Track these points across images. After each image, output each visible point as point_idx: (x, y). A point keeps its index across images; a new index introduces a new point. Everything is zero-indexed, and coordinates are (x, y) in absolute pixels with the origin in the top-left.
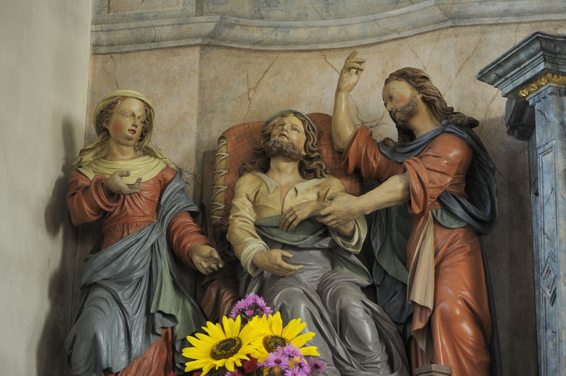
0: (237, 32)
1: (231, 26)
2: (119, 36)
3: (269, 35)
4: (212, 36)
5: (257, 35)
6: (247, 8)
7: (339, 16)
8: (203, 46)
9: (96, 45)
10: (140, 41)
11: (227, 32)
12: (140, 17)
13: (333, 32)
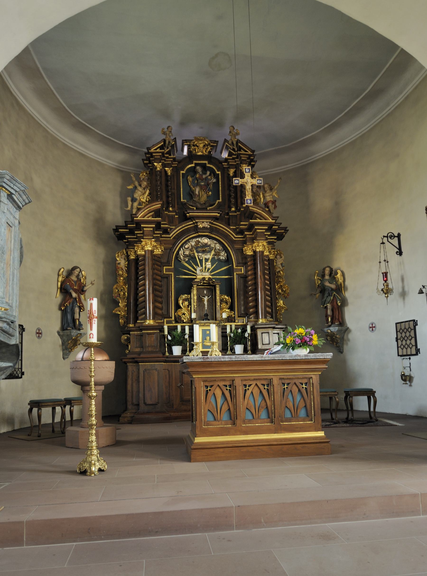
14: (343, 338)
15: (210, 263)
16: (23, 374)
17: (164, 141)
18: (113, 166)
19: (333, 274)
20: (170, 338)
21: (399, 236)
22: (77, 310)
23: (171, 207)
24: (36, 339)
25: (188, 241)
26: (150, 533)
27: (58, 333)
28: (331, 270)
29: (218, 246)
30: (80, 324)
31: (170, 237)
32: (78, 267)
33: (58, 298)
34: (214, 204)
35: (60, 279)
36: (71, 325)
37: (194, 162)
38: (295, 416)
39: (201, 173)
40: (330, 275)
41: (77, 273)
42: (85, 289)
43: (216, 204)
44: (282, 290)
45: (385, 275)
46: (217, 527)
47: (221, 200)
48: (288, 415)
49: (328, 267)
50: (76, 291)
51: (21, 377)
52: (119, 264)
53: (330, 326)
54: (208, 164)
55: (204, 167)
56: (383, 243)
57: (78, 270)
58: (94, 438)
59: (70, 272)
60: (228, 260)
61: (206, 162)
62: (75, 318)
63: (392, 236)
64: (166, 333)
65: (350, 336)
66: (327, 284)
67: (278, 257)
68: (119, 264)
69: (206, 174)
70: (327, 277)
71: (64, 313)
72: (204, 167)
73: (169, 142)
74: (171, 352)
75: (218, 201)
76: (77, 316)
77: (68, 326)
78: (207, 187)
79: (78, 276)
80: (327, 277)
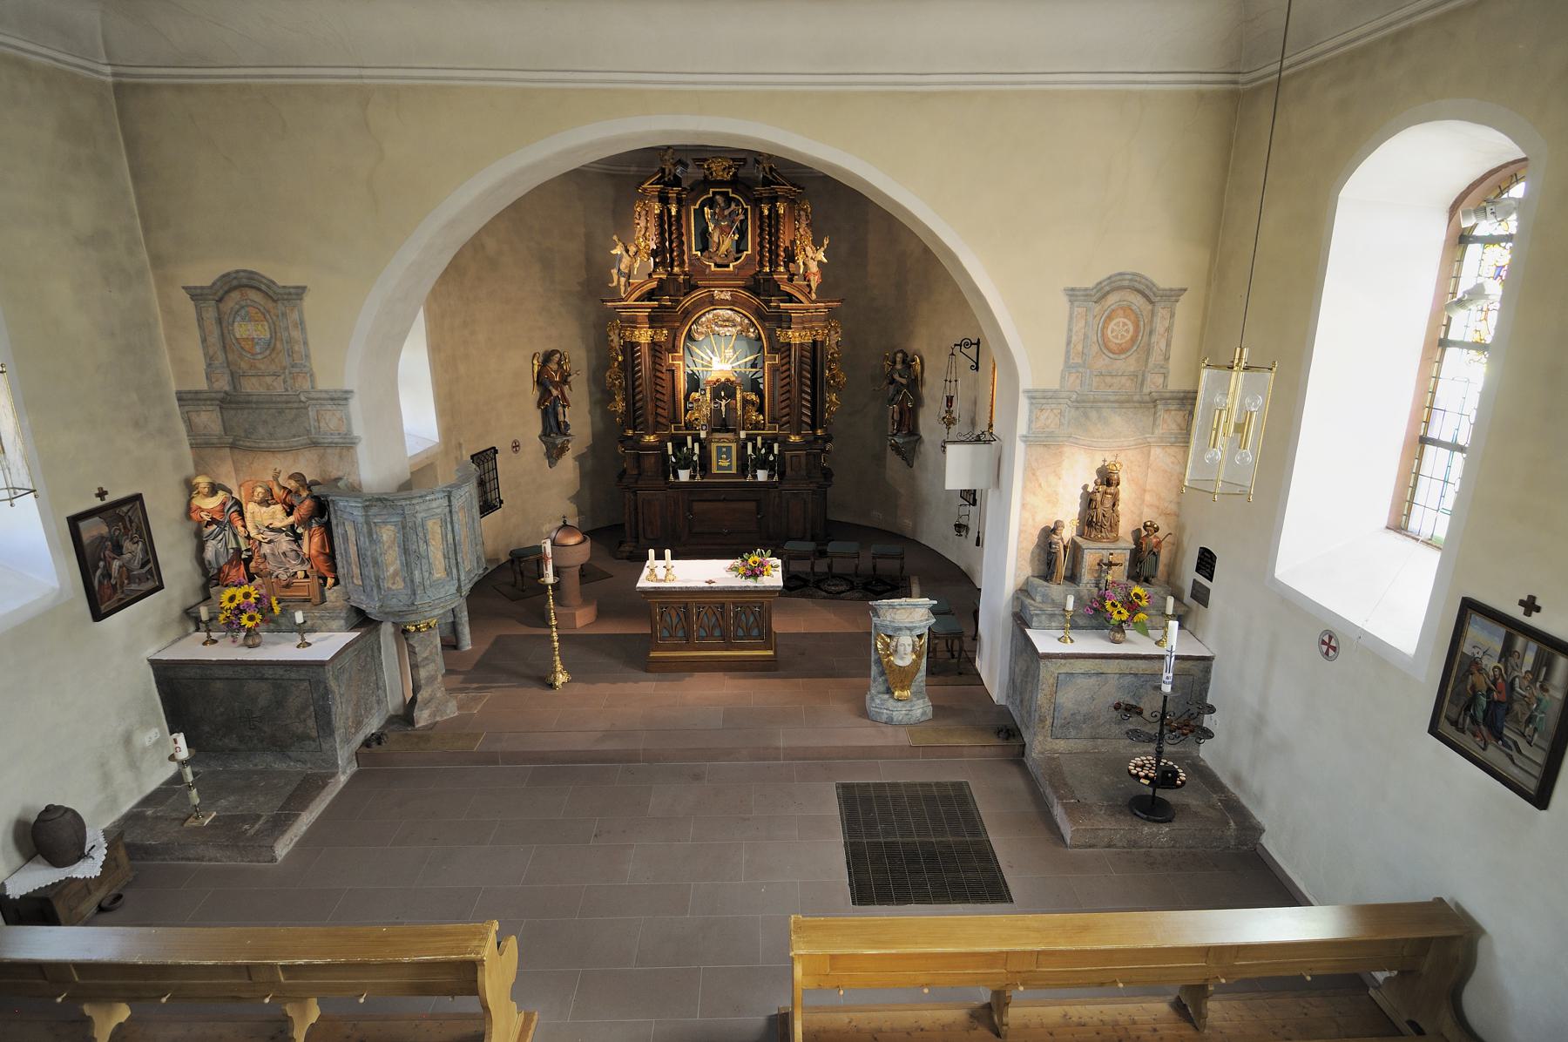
0: (241, 443)
1: (239, 440)
2: (199, 441)
3: (253, 445)
4: (232, 443)
5: (248, 444)
6: (243, 435)
7: (276, 439)
8: (231, 448)
9: (190, 444)
10: (206, 444)
11: (237, 443)
12: (205, 435)
13: (275, 445)
14: (914, 449)
15: (731, 351)
16: (501, 502)
17: (663, 171)
18: (599, 171)
19: (907, 363)
20: (674, 460)
21: (978, 344)
22: (560, 409)
23: (678, 266)
24: (514, 454)
25: (704, 314)
26: (581, 762)
27: (540, 437)
28: (905, 355)
29: (746, 321)
30: (567, 425)
31: (677, 312)
32: (558, 351)
33: (533, 394)
34: (740, 258)
35: (536, 371)
36: (555, 430)
37: (711, 190)
38: (749, 636)
39: (722, 205)
40: (904, 361)
41: (557, 359)
42: (569, 379)
43: (743, 258)
44: (834, 381)
45: (950, 400)
46: (629, 761)
47: (749, 252)
48: (740, 632)
49: (902, 351)
50: (556, 385)
51: (500, 507)
52: (612, 341)
53: (895, 435)
54: (733, 193)
55: (725, 194)
56: (953, 354)
57: (558, 355)
58: (558, 658)
59: (548, 357)
60: (759, 338)
61: (730, 190)
62: (560, 420)
63: (969, 344)
64: (670, 452)
65: (922, 449)
66: (896, 377)
67: (832, 332)
68: (612, 341)
69: (730, 207)
70: (899, 366)
71: (545, 414)
72: (725, 194)
73: (670, 170)
74: (676, 476)
75: (745, 253)
76: (561, 418)
77: (551, 431)
78: (732, 228)
79: (559, 363)
80: (899, 366)
